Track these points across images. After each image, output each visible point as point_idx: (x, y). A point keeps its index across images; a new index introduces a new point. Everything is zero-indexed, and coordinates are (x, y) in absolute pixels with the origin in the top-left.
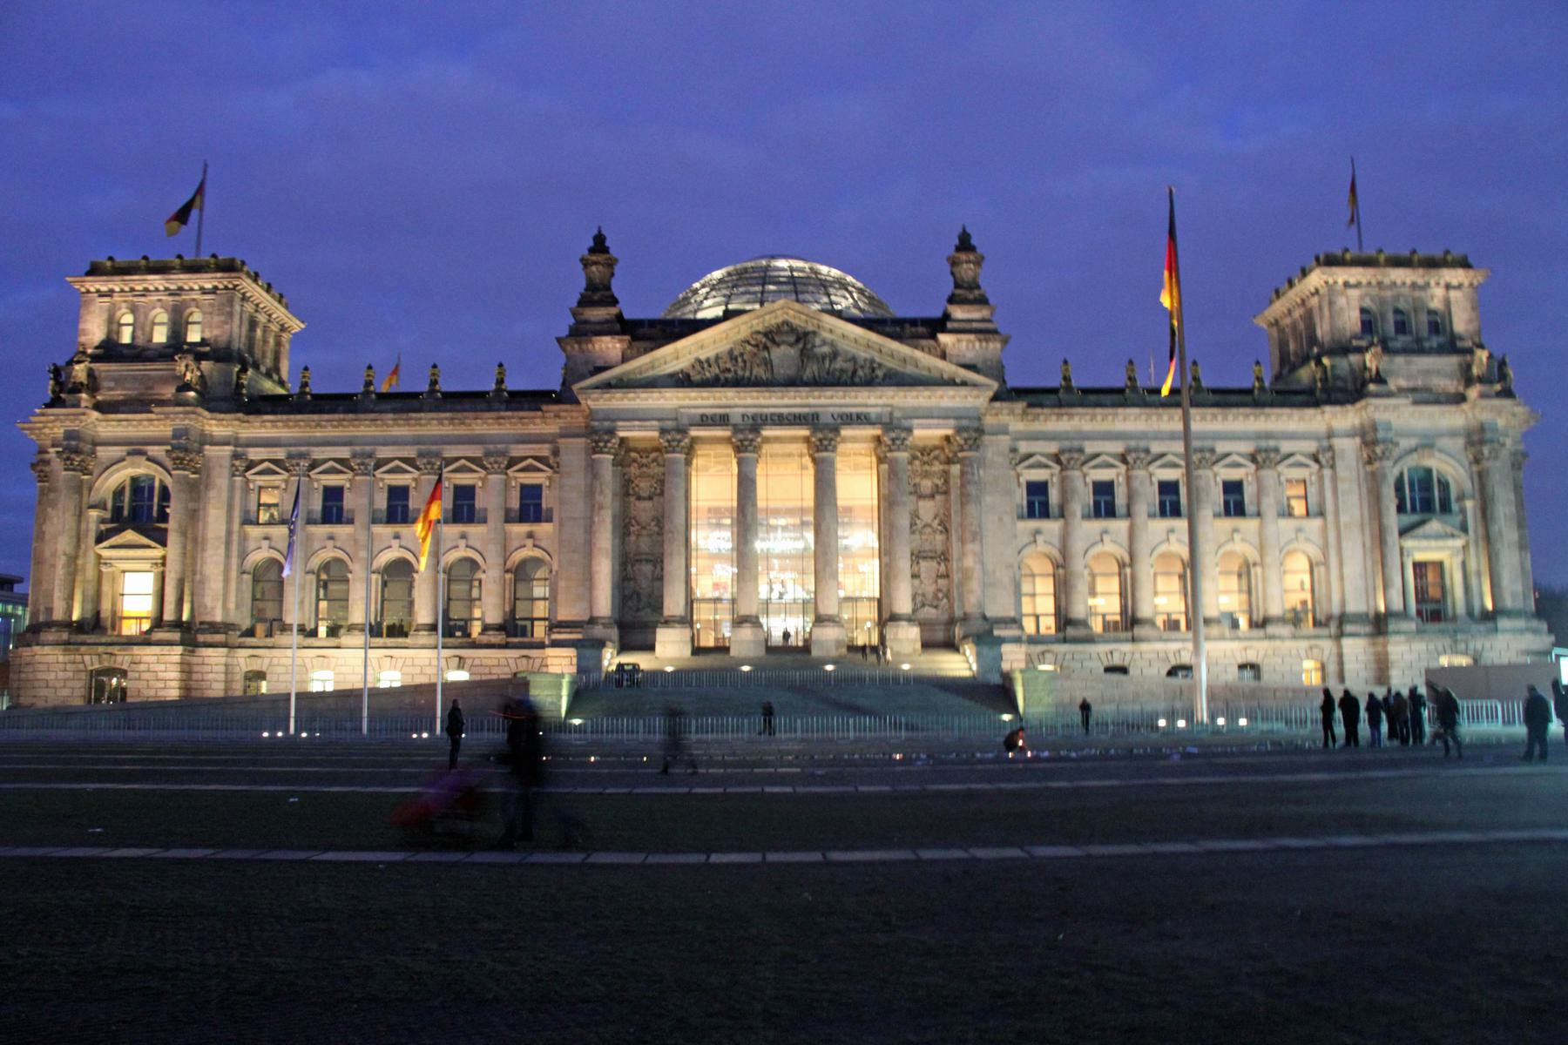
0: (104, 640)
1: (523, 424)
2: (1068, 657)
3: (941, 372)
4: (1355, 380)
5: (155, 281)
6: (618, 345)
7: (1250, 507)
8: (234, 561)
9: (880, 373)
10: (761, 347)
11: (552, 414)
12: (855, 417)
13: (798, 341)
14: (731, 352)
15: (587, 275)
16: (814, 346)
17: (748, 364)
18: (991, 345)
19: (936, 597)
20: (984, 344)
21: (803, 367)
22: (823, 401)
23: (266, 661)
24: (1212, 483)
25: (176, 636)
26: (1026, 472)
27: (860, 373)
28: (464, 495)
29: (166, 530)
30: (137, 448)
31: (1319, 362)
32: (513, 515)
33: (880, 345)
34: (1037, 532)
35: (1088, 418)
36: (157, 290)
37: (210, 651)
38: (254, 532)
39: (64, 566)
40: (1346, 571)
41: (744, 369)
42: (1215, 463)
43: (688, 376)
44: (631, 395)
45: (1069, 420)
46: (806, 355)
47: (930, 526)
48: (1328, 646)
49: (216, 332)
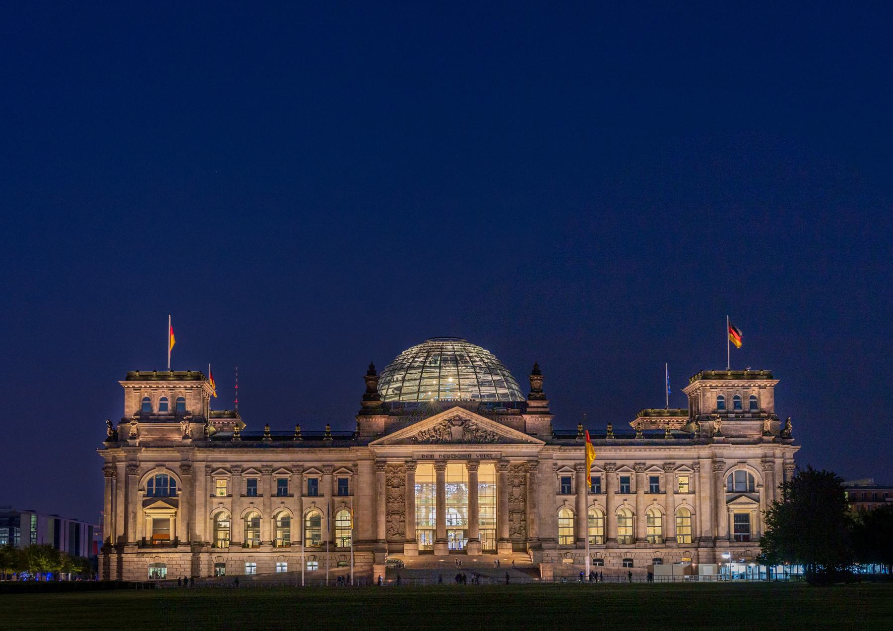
1: (340, 453)
3: (522, 437)
4: (711, 432)
5: (164, 384)
6: (383, 419)
7: (662, 489)
8: (208, 514)
10: (447, 426)
12: (486, 456)
13: (462, 423)
14: (434, 428)
15: (367, 385)
16: (469, 426)
17: (442, 434)
18: (546, 419)
19: (520, 528)
20: (543, 419)
22: (472, 450)
23: (225, 559)
24: (645, 478)
25: (189, 549)
26: (560, 473)
27: (488, 437)
28: (314, 483)
30: (160, 464)
31: (697, 424)
32: (335, 492)
34: (565, 501)
36: (163, 387)
38: (215, 500)
39: (132, 519)
40: (702, 517)
43: (416, 438)
45: (580, 451)
46: (466, 430)
47: (517, 499)
48: (693, 551)
49: (194, 408)
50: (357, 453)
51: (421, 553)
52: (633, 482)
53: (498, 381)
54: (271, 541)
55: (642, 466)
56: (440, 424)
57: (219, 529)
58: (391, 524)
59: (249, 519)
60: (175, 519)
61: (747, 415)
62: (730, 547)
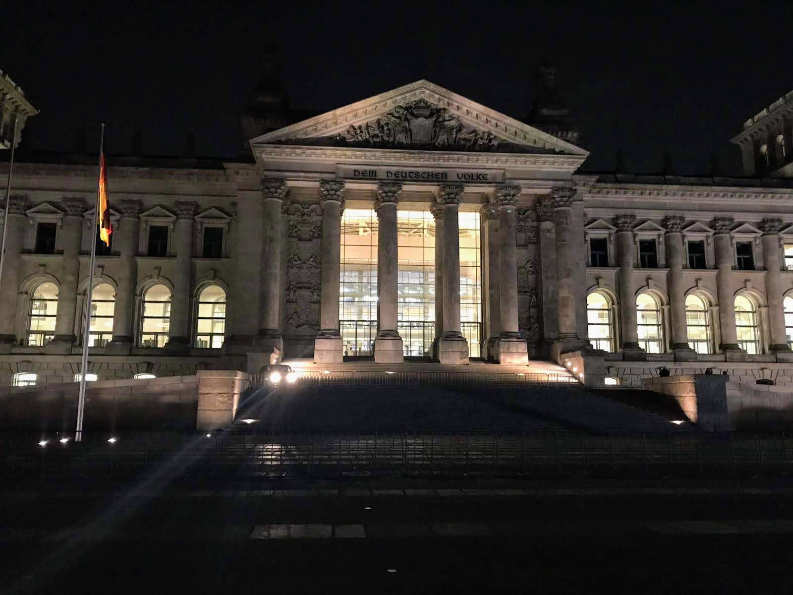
2: (628, 371)
7: (758, 263)
9: (495, 143)
10: (403, 119)
12: (475, 177)
13: (431, 115)
14: (378, 121)
16: (445, 120)
17: (392, 132)
21: (435, 135)
22: (451, 163)
27: (480, 142)
33: (498, 120)
41: (389, 135)
43: (344, 138)
44: (298, 151)
45: (625, 193)
46: (439, 125)
47: (525, 267)
51: (347, 359)
52: (709, 251)
55: (727, 223)
56: (392, 114)
58: (293, 305)
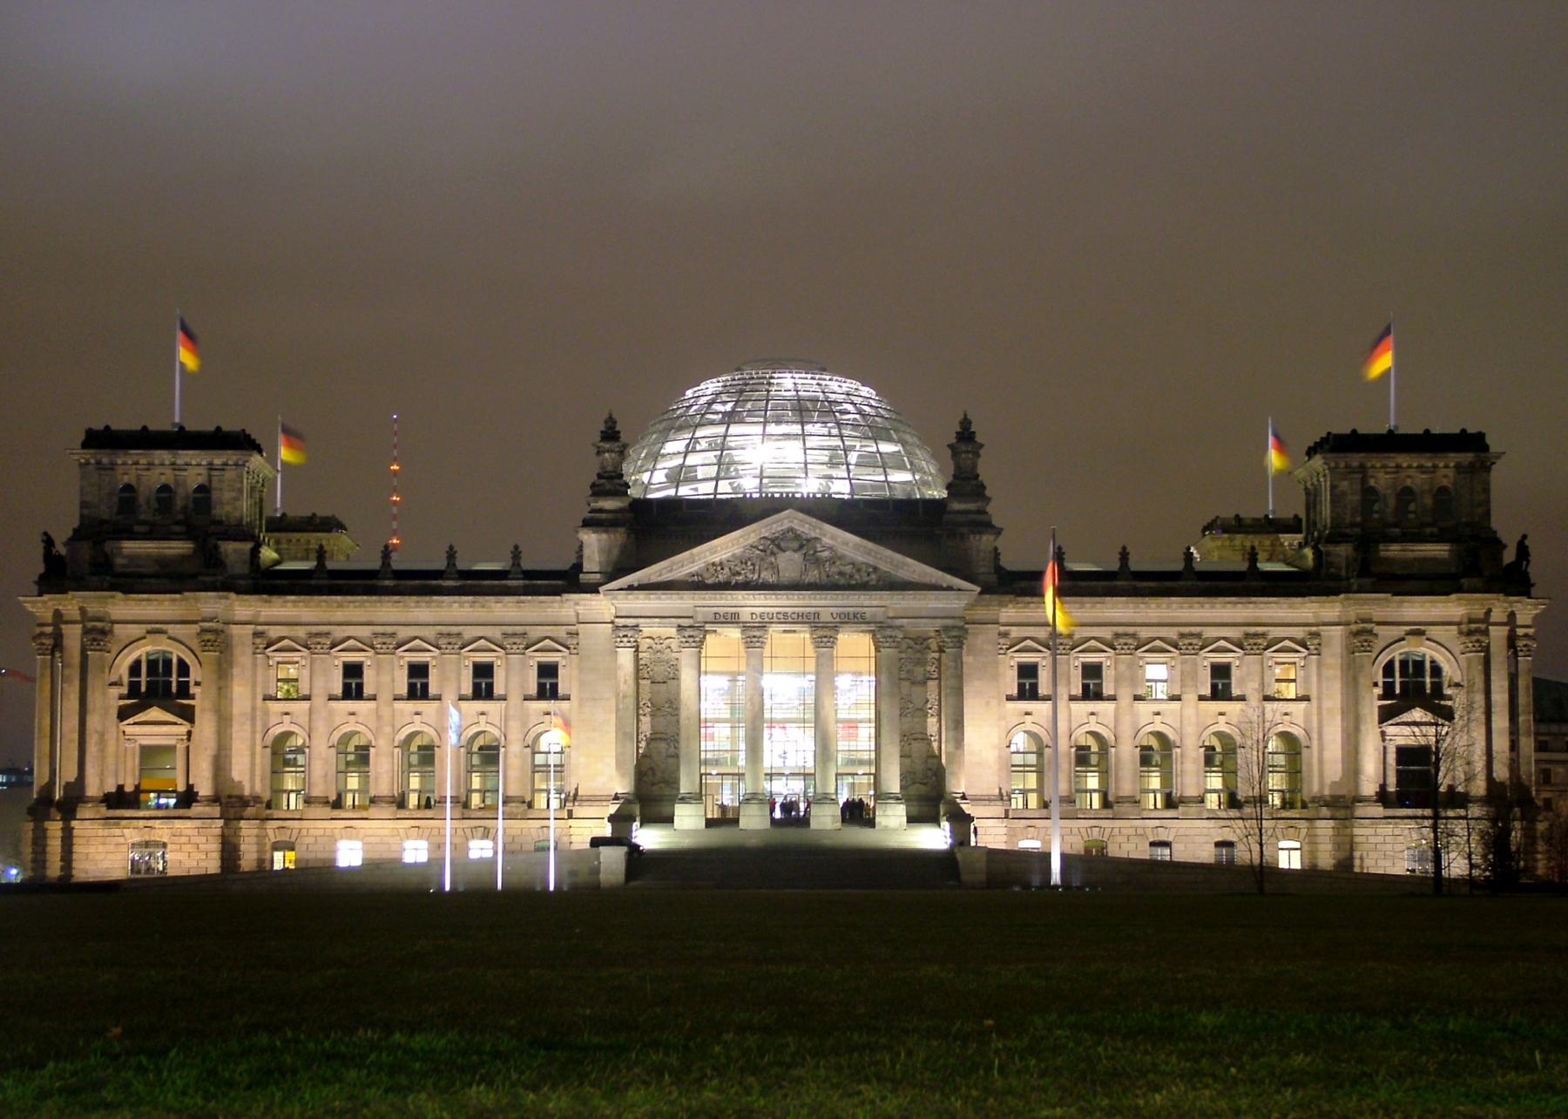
0: (141, 813)
7: (1235, 692)
8: (259, 736)
10: (768, 552)
11: (572, 603)
12: (851, 616)
13: (801, 547)
16: (816, 552)
17: (757, 568)
23: (295, 832)
29: (193, 707)
30: (156, 629)
35: (1077, 606)
37: (243, 823)
42: (1202, 648)
48: (1303, 824)
50: (578, 607)
53: (892, 454)
54: (393, 796)
55: (1194, 641)
56: (756, 547)
57: (288, 769)
59: (351, 749)
60: (188, 747)
61: (1428, 530)
62: (1385, 818)
